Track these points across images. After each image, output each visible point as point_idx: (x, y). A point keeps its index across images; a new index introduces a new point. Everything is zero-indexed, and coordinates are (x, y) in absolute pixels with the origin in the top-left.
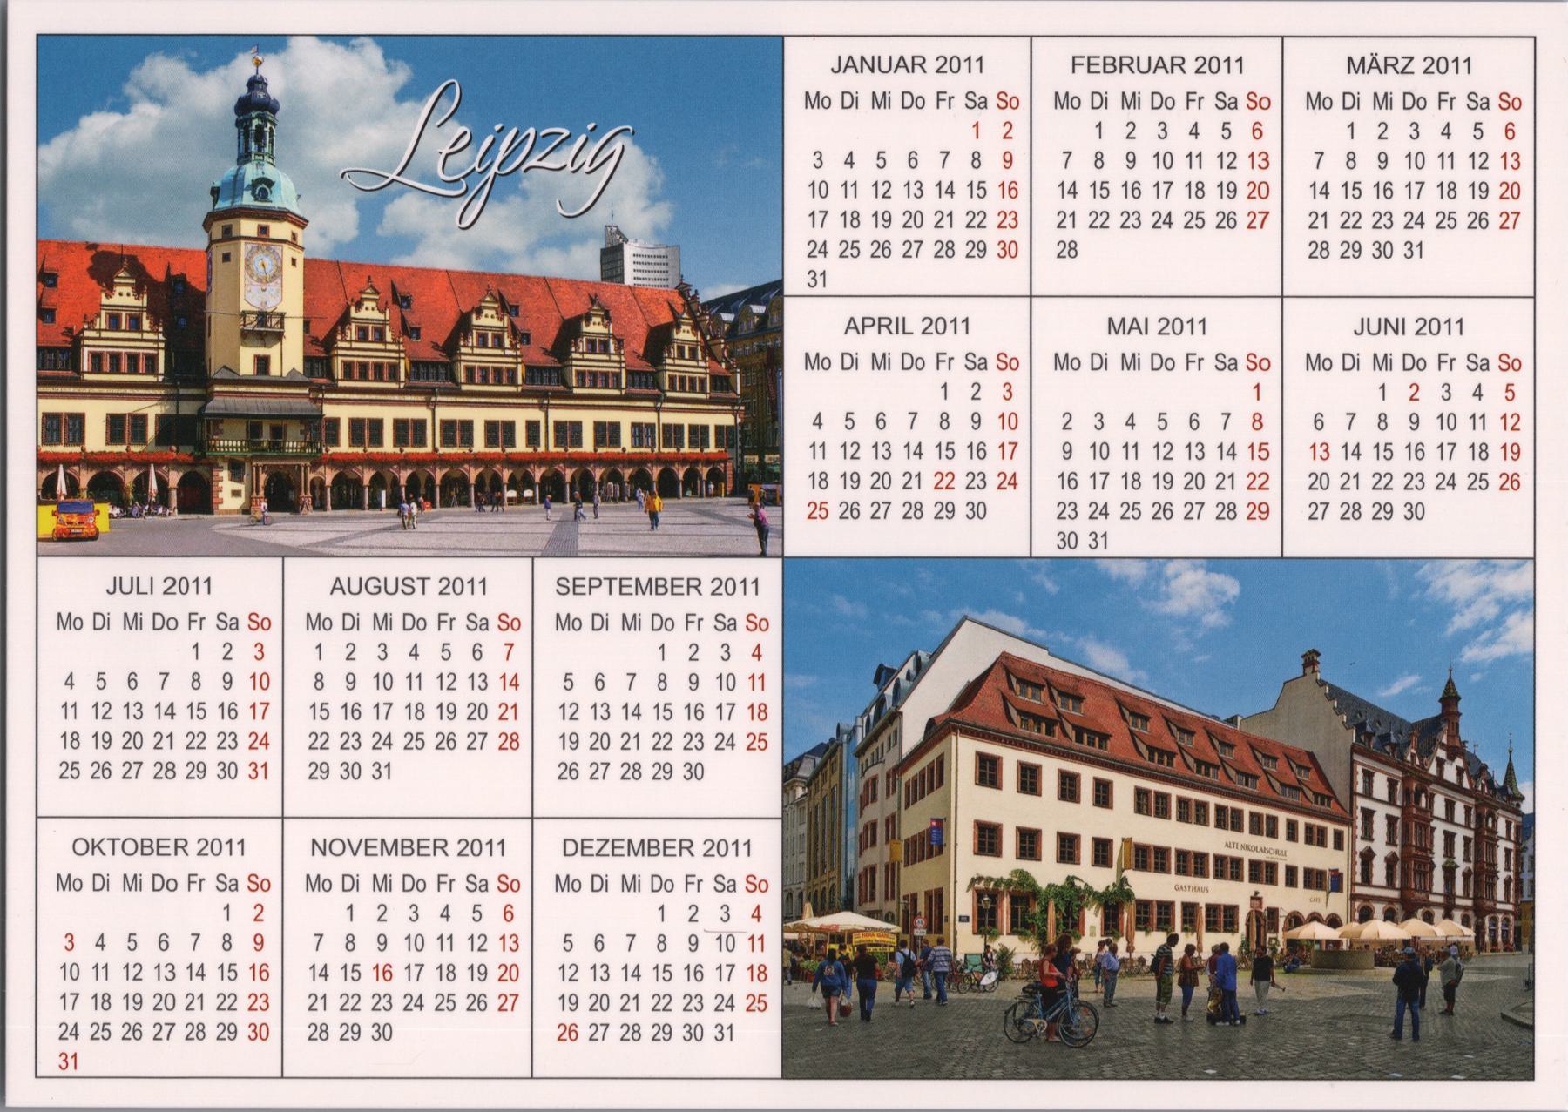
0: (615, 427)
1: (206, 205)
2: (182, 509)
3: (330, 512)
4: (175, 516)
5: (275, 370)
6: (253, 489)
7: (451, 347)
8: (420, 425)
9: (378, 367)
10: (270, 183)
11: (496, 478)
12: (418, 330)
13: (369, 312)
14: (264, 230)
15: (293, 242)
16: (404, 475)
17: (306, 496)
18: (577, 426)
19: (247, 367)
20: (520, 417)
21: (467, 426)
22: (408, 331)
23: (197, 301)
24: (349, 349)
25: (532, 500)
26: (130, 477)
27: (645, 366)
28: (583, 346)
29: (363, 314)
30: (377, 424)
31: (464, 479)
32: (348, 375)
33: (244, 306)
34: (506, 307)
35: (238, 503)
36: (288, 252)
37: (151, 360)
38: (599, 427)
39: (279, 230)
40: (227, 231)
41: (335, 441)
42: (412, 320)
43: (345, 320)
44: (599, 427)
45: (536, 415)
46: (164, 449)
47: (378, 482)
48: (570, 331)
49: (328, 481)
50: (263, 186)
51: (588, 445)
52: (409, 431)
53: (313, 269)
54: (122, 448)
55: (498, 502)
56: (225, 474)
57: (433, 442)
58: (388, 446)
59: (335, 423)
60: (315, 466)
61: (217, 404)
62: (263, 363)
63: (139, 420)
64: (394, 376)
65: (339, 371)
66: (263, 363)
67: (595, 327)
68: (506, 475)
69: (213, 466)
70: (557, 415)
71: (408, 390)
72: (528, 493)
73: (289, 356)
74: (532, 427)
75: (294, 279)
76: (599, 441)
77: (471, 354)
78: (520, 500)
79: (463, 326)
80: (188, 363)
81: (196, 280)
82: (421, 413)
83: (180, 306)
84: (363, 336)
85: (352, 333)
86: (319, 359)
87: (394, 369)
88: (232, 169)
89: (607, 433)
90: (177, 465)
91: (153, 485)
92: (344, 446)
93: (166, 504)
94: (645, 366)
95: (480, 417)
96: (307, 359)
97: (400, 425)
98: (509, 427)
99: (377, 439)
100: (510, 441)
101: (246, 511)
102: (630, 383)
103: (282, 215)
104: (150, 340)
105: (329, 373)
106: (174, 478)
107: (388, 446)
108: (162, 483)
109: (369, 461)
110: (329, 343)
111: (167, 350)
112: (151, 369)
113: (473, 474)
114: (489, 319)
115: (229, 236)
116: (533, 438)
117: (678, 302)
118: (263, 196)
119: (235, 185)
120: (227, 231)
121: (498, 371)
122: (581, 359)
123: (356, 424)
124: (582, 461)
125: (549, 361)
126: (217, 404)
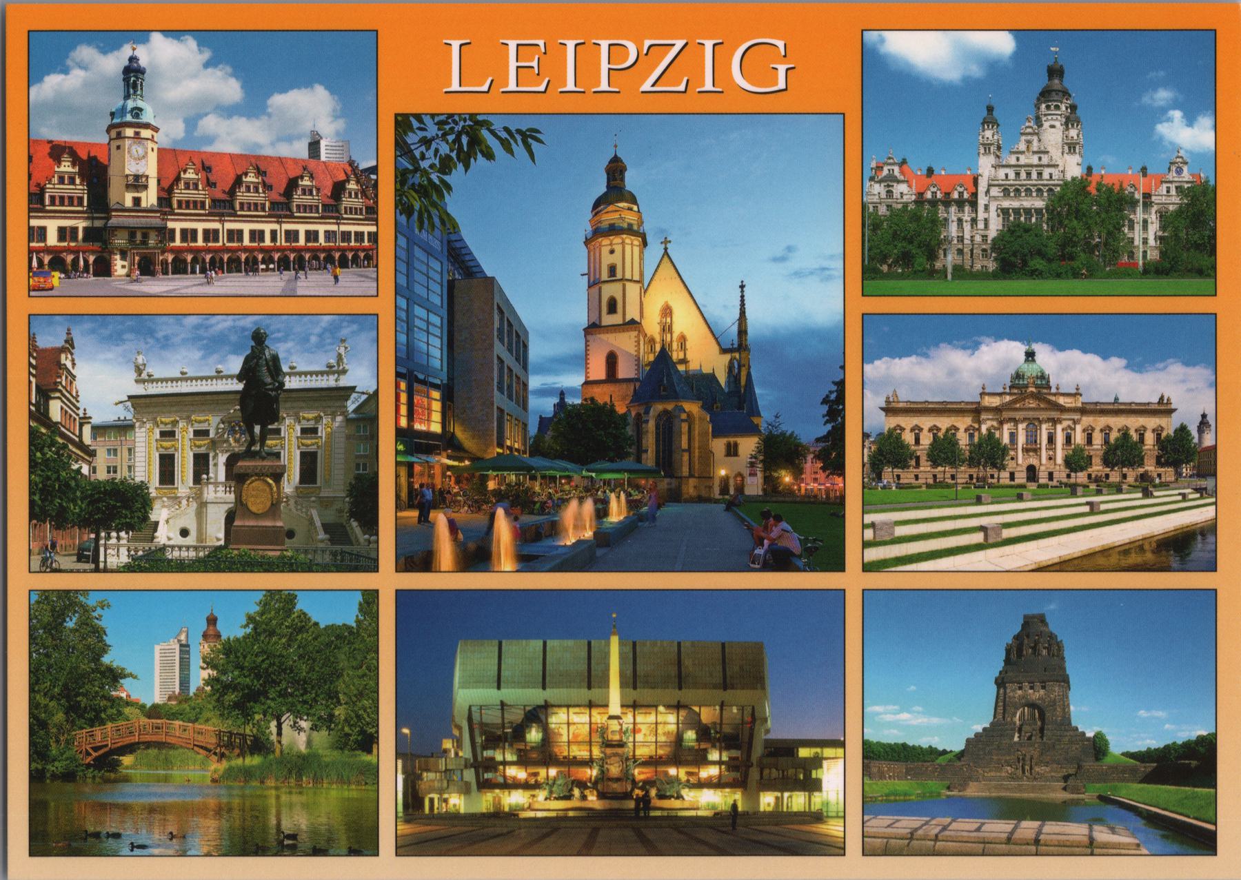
0: (316, 233)
1: (108, 121)
2: (95, 275)
3: (170, 276)
4: (93, 278)
5: (144, 204)
7: (232, 192)
8: (216, 231)
9: (195, 202)
10: (141, 110)
11: (255, 259)
12: (215, 184)
13: (190, 175)
14: (137, 133)
15: (152, 139)
16: (208, 257)
17: (158, 268)
18: (297, 232)
19: (129, 203)
20: (267, 228)
21: (240, 232)
22: (210, 184)
24: (180, 194)
25: (273, 270)
26: (69, 258)
27: (332, 202)
28: (299, 192)
29: (187, 176)
30: (195, 231)
31: (239, 259)
32: (180, 207)
33: (127, 172)
34: (260, 172)
35: (124, 271)
36: (150, 145)
37: (81, 199)
38: (308, 233)
39: (146, 133)
41: (173, 240)
42: (212, 179)
43: (178, 179)
44: (308, 233)
45: (276, 226)
46: (86, 244)
47: (195, 260)
48: (292, 184)
49: (170, 260)
50: (137, 111)
51: (302, 241)
52: (210, 235)
53: (162, 153)
54: (65, 244)
55: (256, 270)
56: (118, 257)
58: (200, 242)
59: (173, 231)
60: (163, 252)
61: (113, 222)
62: (137, 201)
64: (203, 207)
65: (175, 206)
66: (137, 201)
67: (306, 182)
68: (260, 257)
69: (111, 253)
70: (286, 227)
72: (271, 266)
73: (150, 198)
74: (274, 233)
75: (153, 158)
76: (308, 239)
77: (242, 196)
78: (267, 270)
79: (238, 181)
80: (99, 201)
81: (103, 159)
82: (216, 225)
83: (95, 172)
84: (187, 187)
85: (182, 185)
86: (165, 199)
87: (203, 203)
88: (121, 103)
89: (312, 236)
90: (93, 252)
91: (82, 263)
92: (178, 242)
93: (88, 272)
95: (246, 228)
96: (159, 199)
97: (206, 232)
98: (262, 232)
99: (195, 239)
101: (128, 275)
102: (324, 210)
103: (147, 126)
104: (79, 189)
105: (170, 206)
106: (92, 259)
107: (200, 242)
108: (86, 261)
109: (190, 250)
110: (170, 191)
111: (88, 194)
112: (80, 203)
113: (243, 257)
114: (251, 178)
115: (120, 136)
116: (274, 238)
118: (137, 116)
119: (123, 110)
121: (256, 205)
122: (298, 198)
123: (184, 231)
125: (282, 199)
126: (113, 222)
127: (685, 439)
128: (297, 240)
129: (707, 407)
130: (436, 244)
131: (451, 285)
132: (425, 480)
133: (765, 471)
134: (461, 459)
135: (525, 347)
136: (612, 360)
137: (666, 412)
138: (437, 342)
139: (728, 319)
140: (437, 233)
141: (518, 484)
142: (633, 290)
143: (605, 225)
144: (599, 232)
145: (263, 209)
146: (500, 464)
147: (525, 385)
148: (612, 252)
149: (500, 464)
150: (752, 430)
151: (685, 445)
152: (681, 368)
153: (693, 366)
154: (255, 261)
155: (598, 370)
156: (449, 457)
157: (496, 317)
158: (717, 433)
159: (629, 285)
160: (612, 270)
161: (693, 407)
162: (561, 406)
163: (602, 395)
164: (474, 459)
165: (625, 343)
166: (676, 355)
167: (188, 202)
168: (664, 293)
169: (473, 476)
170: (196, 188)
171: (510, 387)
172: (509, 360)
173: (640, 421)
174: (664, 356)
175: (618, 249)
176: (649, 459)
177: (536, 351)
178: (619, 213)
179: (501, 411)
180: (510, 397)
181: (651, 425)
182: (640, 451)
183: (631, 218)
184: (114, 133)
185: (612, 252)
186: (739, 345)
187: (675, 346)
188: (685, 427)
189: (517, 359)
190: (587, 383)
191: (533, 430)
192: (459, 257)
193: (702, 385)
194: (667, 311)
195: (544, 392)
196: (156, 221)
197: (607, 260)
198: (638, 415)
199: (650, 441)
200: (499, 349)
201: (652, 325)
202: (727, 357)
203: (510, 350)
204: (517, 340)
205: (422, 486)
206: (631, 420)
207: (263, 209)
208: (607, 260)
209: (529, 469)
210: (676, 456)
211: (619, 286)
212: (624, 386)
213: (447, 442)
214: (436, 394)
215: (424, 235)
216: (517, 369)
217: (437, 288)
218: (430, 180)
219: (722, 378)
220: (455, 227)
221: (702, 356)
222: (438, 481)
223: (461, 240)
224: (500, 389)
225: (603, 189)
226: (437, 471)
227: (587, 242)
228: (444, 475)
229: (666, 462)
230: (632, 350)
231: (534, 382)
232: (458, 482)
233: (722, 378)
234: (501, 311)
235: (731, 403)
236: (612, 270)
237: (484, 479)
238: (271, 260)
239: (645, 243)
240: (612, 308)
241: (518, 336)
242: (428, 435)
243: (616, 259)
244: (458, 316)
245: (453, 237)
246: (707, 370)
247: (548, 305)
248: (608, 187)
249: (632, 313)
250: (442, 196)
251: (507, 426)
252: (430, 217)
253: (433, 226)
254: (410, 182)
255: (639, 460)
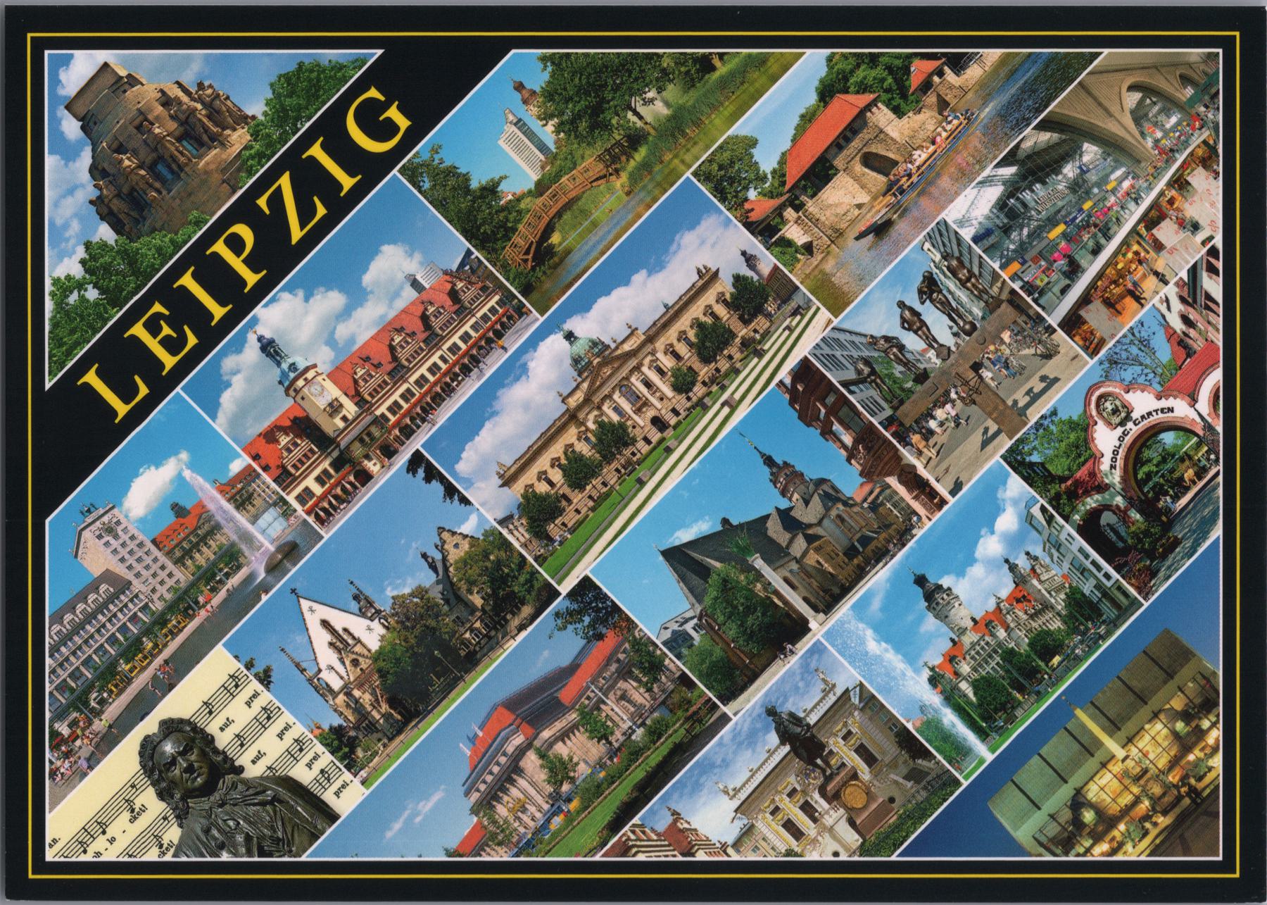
0: (466, 333)
1: (281, 389)
2: (363, 486)
4: (363, 489)
5: (350, 417)
6: (378, 458)
7: (395, 358)
8: (408, 390)
9: (379, 386)
11: (446, 384)
13: (360, 372)
15: (318, 374)
16: (418, 410)
18: (455, 344)
19: (341, 425)
20: (435, 358)
21: (422, 376)
22: (377, 366)
23: (307, 418)
26: (339, 491)
27: (456, 307)
30: (396, 403)
31: (437, 393)
32: (373, 397)
34: (399, 330)
35: (378, 466)
36: (319, 378)
37: (311, 450)
38: (461, 338)
39: (310, 375)
40: (295, 390)
41: (388, 420)
43: (356, 382)
44: (461, 338)
45: (439, 353)
47: (412, 419)
48: (424, 318)
50: (293, 367)
51: (463, 347)
52: (407, 396)
55: (454, 389)
57: (417, 392)
58: (405, 406)
60: (390, 433)
61: (343, 444)
62: (344, 419)
63: (325, 472)
65: (369, 398)
66: (344, 419)
67: (431, 309)
68: (448, 380)
69: (360, 463)
70: (445, 347)
71: (395, 384)
73: (350, 409)
74: (442, 358)
76: (465, 342)
77: (403, 355)
78: (459, 383)
79: (392, 349)
80: (323, 441)
81: (301, 414)
82: (405, 386)
83: (304, 426)
85: (362, 383)
86: (360, 402)
87: (384, 382)
88: (278, 371)
89: (466, 337)
90: (349, 473)
91: (348, 486)
92: (393, 419)
93: (355, 488)
94: (456, 307)
95: (423, 370)
97: (402, 396)
98: (435, 364)
99: (400, 407)
100: (439, 369)
103: (307, 369)
104: (304, 444)
105: (367, 402)
106: (352, 478)
107: (405, 406)
108: (350, 483)
109: (404, 416)
110: (358, 393)
113: (438, 389)
114: (398, 339)
117: (448, 278)
118: (296, 369)
119: (283, 372)
120: (295, 390)
122: (436, 324)
123: (390, 409)
124: (466, 353)
125: (427, 334)
126: (343, 444)
128: (459, 349)
145: (423, 350)
154: (448, 385)
167: (375, 390)
170: (372, 377)
184: (292, 393)
196: (369, 419)
207: (423, 350)
238: (457, 375)
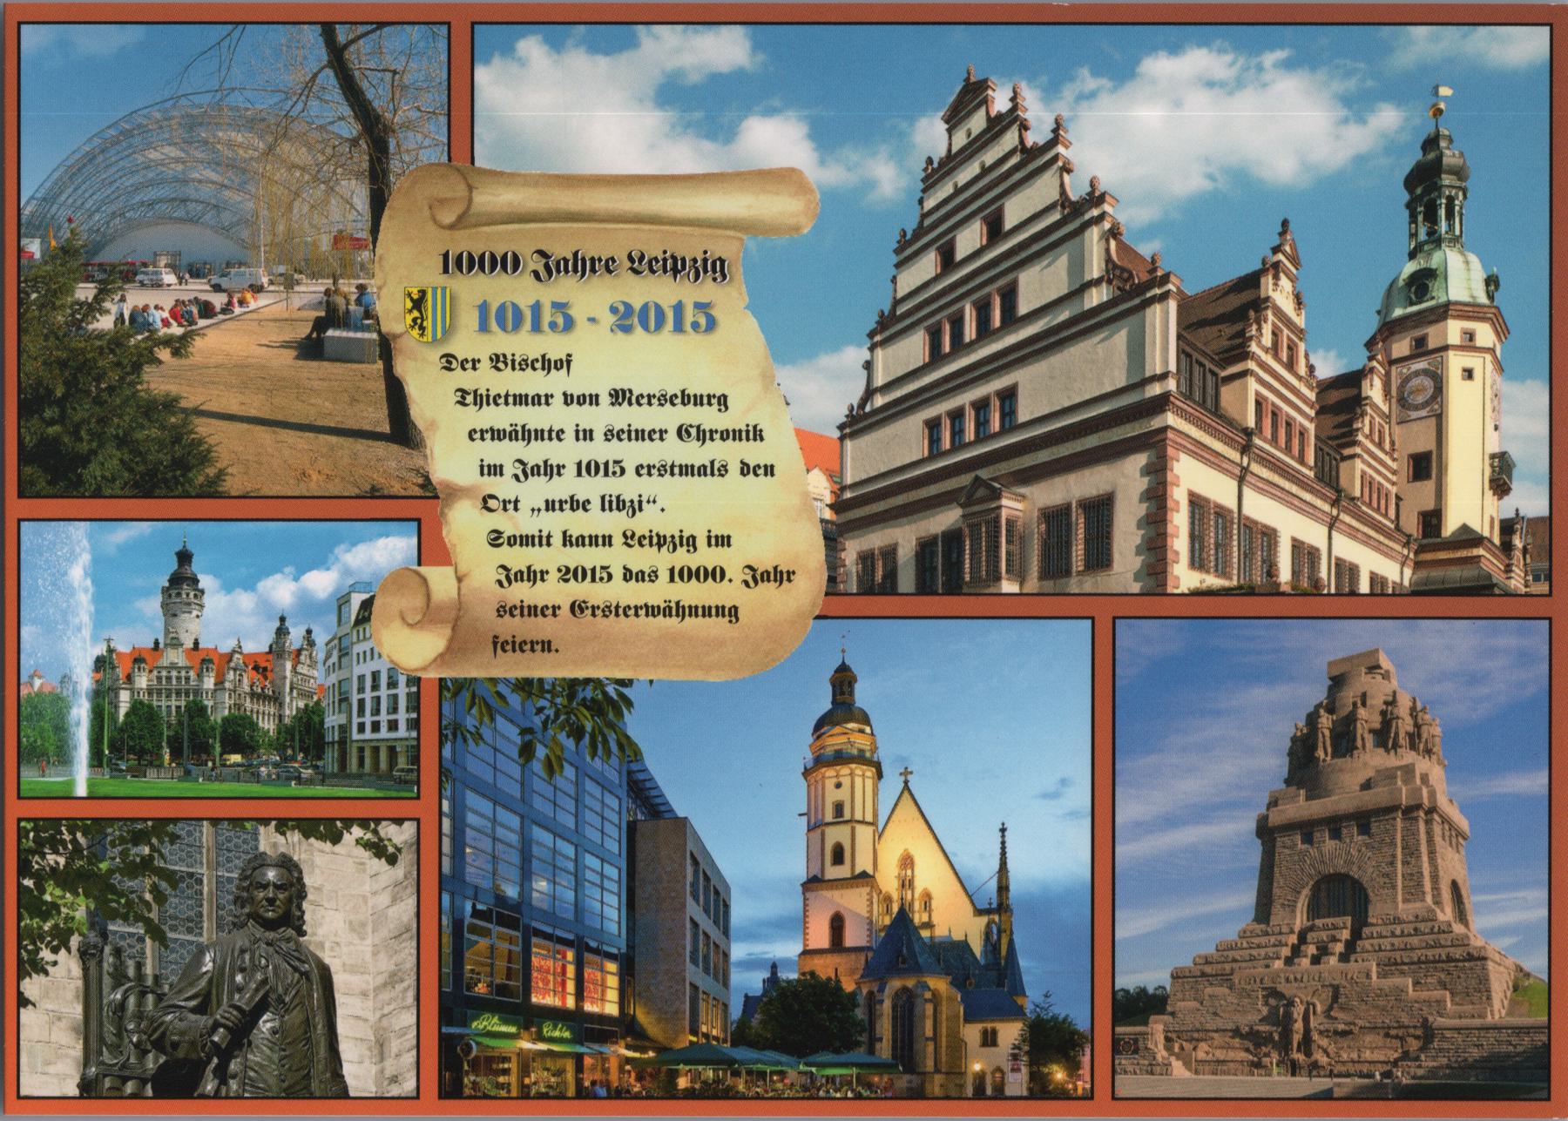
127: (929, 1024)
129: (958, 983)
130: (613, 776)
131: (632, 828)
132: (598, 1076)
133: (1031, 1064)
134: (643, 1050)
135: (727, 906)
136: (837, 924)
137: (905, 989)
138: (612, 900)
139: (984, 870)
140: (614, 761)
141: (717, 1081)
142: (864, 834)
143: (829, 751)
144: (820, 762)
146: (694, 1056)
147: (726, 955)
148: (838, 786)
149: (694, 1056)
150: (1016, 1012)
151: (929, 1032)
152: (925, 934)
153: (940, 932)
155: (820, 937)
156: (628, 1047)
157: (689, 870)
158: (970, 1018)
159: (860, 829)
160: (839, 808)
161: (939, 984)
162: (773, 981)
163: (825, 967)
164: (661, 1049)
165: (854, 902)
166: (918, 918)
168: (904, 837)
169: (659, 1071)
171: (706, 957)
172: (706, 924)
173: (872, 1001)
174: (903, 918)
175: (846, 782)
176: (884, 1051)
177: (740, 912)
178: (846, 737)
179: (694, 987)
180: (706, 970)
181: (887, 1006)
182: (873, 1040)
183: (861, 742)
185: (838, 786)
186: (998, 906)
187: (917, 906)
188: (929, 1008)
189: (716, 922)
190: (806, 953)
191: (736, 1012)
192: (642, 794)
193: (951, 955)
194: (907, 861)
195: (750, 964)
197: (832, 795)
198: (871, 993)
199: (885, 1027)
200: (693, 910)
201: (888, 880)
202: (984, 920)
203: (706, 911)
204: (717, 902)
205: (593, 1083)
206: (861, 1000)
208: (832, 795)
209: (730, 1062)
210: (917, 1046)
211: (846, 829)
212: (853, 956)
213: (625, 1027)
214: (612, 967)
215: (598, 763)
216: (715, 934)
217: (614, 832)
218: (605, 694)
219: (977, 947)
220: (637, 754)
221: (952, 918)
222: (614, 1077)
223: (645, 770)
224: (694, 961)
225: (826, 705)
226: (613, 1065)
227: (807, 773)
228: (621, 1070)
229: (905, 1054)
230: (863, 910)
231: (738, 951)
232: (639, 1078)
233: (977, 947)
234: (695, 862)
235: (988, 978)
236: (839, 808)
237: (674, 1074)
239: (880, 775)
240: (838, 856)
241: (717, 892)
242: (602, 1018)
243: (843, 795)
244: (640, 866)
245: (634, 767)
246: (957, 936)
247: (755, 853)
248: (833, 702)
249: (863, 864)
250: (620, 714)
251: (702, 1005)
252: (605, 741)
253: (608, 752)
254: (581, 696)
255: (871, 1051)
